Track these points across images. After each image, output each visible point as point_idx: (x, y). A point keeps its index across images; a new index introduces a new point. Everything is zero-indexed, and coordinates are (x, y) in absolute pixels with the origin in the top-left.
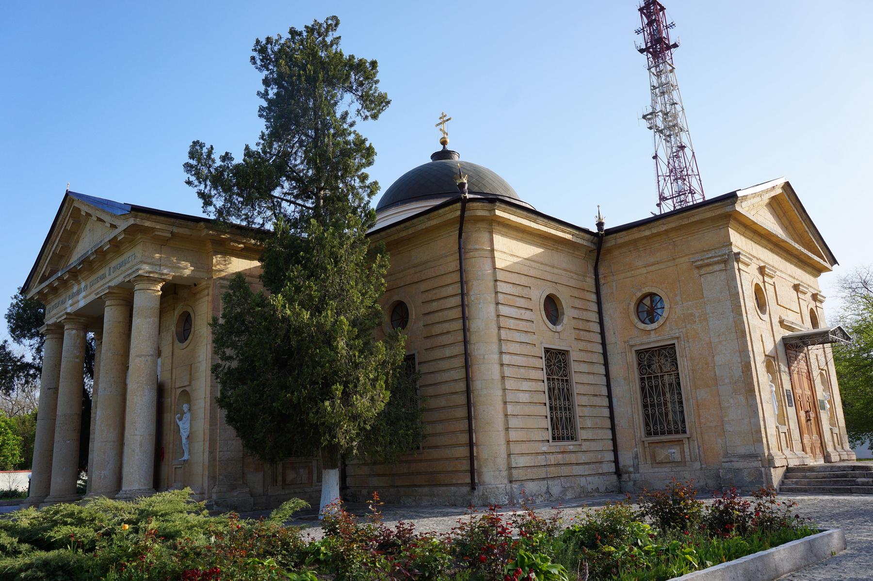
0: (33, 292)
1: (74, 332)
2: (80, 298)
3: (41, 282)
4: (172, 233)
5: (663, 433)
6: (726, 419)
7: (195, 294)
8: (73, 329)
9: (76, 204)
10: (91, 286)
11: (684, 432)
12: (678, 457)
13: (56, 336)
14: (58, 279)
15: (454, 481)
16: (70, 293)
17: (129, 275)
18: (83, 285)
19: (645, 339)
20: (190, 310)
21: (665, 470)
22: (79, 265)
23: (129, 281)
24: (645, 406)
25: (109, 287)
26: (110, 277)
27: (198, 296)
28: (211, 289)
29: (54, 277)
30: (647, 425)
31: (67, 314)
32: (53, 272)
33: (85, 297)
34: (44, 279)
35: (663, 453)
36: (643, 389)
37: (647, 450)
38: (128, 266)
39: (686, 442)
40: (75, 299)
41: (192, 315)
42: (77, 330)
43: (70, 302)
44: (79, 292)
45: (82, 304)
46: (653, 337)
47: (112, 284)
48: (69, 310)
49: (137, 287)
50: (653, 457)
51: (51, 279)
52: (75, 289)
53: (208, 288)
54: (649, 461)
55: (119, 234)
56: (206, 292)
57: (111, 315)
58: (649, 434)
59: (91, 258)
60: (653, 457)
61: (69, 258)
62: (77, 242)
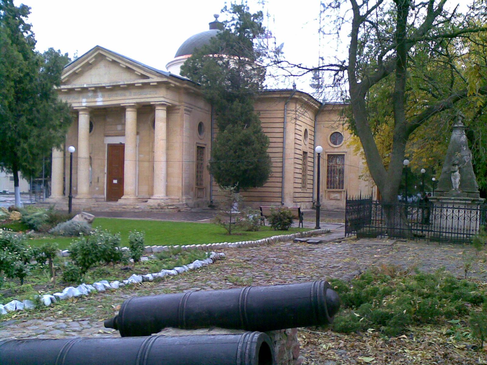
1: (87, 116)
4: (175, 85)
5: (334, 188)
6: (360, 186)
8: (86, 114)
11: (343, 188)
12: (339, 198)
15: (272, 201)
19: (332, 150)
21: (332, 202)
24: (328, 177)
25: (134, 103)
30: (327, 184)
31: (86, 106)
35: (333, 195)
36: (328, 170)
37: (327, 194)
39: (343, 192)
43: (84, 100)
46: (336, 150)
49: (157, 108)
50: (329, 197)
54: (327, 198)
56: (177, 111)
57: (130, 116)
58: (328, 188)
60: (329, 197)
62: (91, 69)
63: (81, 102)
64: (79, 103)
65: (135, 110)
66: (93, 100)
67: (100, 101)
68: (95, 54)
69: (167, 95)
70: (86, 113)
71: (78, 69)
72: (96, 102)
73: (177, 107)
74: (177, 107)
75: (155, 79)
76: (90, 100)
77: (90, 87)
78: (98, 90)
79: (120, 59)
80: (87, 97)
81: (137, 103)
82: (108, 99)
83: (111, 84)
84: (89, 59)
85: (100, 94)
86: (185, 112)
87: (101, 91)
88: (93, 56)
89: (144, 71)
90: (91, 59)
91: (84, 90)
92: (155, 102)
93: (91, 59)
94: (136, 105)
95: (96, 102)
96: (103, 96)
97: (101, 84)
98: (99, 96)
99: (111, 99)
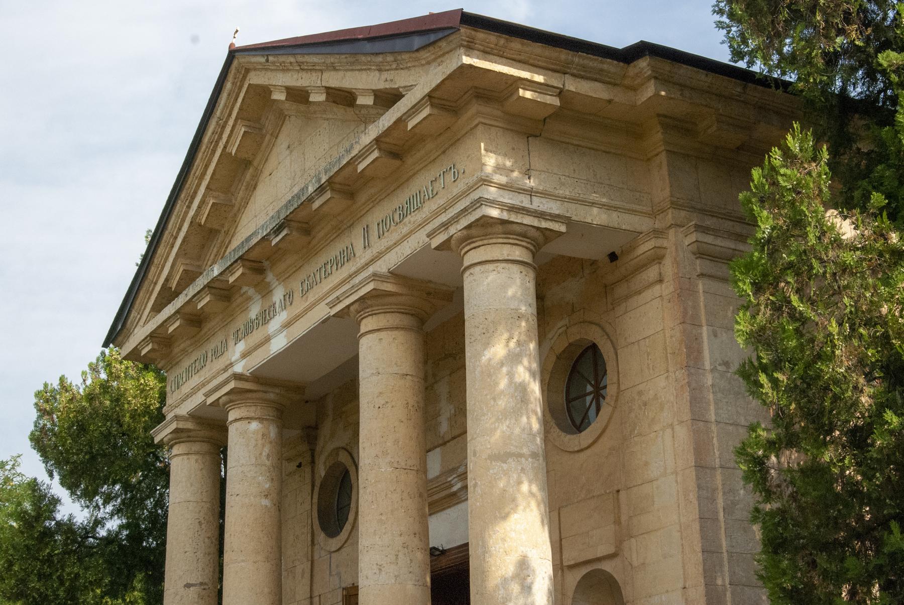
0: (139, 333)
1: (254, 425)
2: (276, 330)
3: (158, 308)
7: (607, 289)
8: (249, 419)
9: (256, 79)
10: (304, 293)
13: (196, 447)
14: (209, 287)
16: (239, 323)
17: (445, 226)
18: (278, 295)
20: (594, 335)
22: (277, 230)
23: (445, 246)
25: (375, 276)
26: (368, 255)
27: (621, 290)
28: (668, 262)
29: (201, 282)
31: (238, 377)
32: (189, 278)
33: (287, 325)
34: (167, 295)
38: (431, 206)
40: (257, 336)
41: (605, 349)
42: (260, 419)
43: (241, 347)
44: (265, 317)
45: (279, 344)
47: (382, 267)
48: (238, 368)
51: (191, 291)
52: (254, 311)
53: (657, 258)
55: (415, 109)
59: (316, 204)
61: (230, 234)
63: (231, 365)
64: (225, 370)
65: (406, 320)
68: (240, 100)
69: (528, 173)
73: (646, 247)
74: (646, 247)
80: (249, 328)
81: (395, 275)
86: (700, 265)
90: (233, 138)
93: (233, 138)
94: (389, 287)
97: (255, 233)
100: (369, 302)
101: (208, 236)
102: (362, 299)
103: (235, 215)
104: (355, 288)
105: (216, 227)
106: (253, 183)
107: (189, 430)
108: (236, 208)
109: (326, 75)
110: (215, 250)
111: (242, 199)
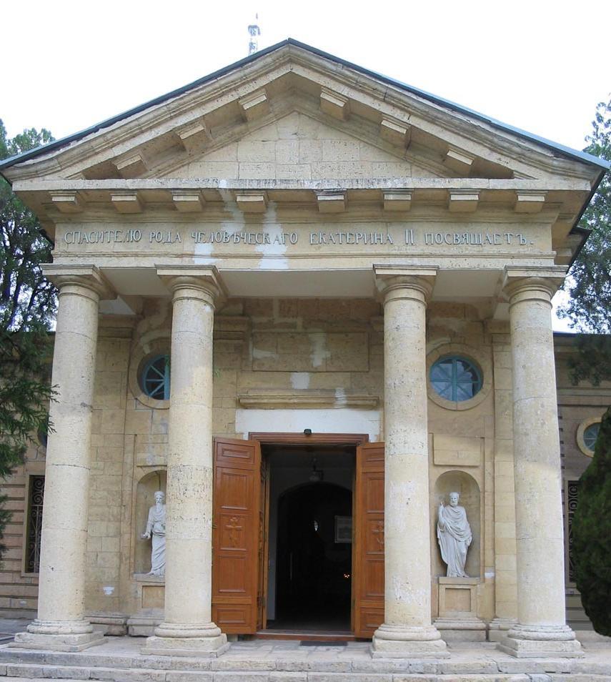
32: (136, 171)
62: (237, 140)
66: (242, 249)
67: (276, 255)
68: (273, 76)
70: (207, 298)
71: (192, 123)
72: (259, 256)
75: (538, 182)
76: (230, 249)
77: (245, 192)
78: (271, 214)
79: (385, 99)
82: (312, 251)
83: (346, 186)
84: (242, 92)
85: (274, 231)
87: (279, 220)
88: (263, 82)
89: (494, 148)
90: (251, 97)
91: (212, 205)
92: (528, 269)
93: (251, 97)
95: (259, 256)
96: (289, 239)
98: (272, 238)
99: (325, 250)
100: (419, 281)
101: (176, 149)
102: (417, 276)
103: (207, 148)
104: (412, 267)
105: (187, 147)
106: (237, 137)
107: (95, 280)
108: (211, 144)
109: (412, 118)
110: (172, 162)
111: (221, 141)
